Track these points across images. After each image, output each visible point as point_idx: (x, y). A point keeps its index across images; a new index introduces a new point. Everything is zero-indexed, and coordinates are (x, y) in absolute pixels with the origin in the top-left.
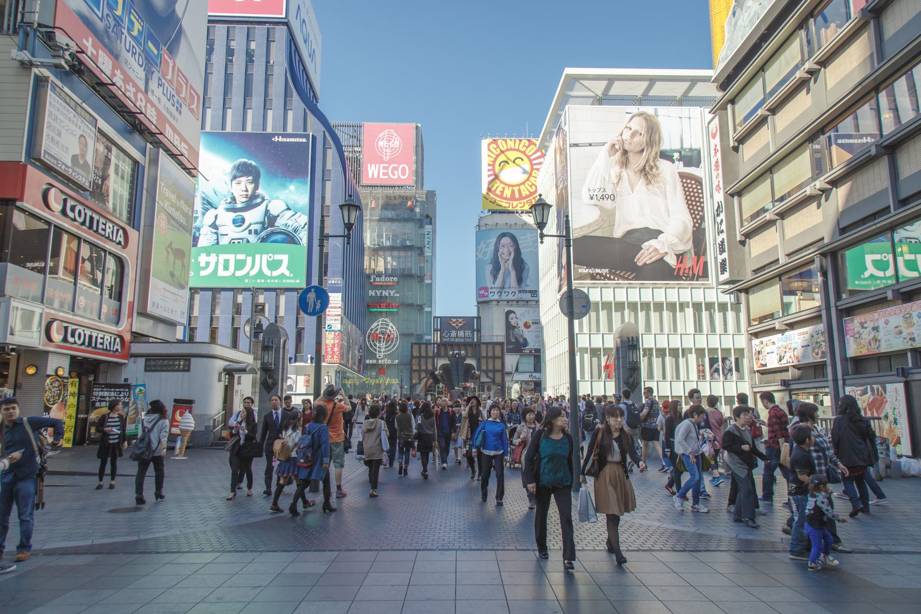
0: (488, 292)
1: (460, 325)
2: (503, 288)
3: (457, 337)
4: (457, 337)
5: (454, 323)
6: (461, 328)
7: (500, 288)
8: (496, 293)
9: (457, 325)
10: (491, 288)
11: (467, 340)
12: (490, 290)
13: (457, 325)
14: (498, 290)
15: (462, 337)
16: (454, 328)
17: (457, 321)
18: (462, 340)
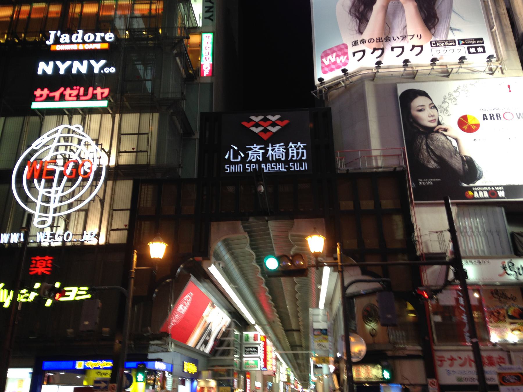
0: (346, 54)
1: (274, 130)
2: (388, 39)
3: (266, 160)
4: (266, 160)
5: (257, 125)
6: (275, 139)
7: (379, 40)
8: (369, 51)
9: (265, 131)
10: (356, 43)
11: (296, 167)
12: (351, 50)
13: (265, 131)
14: (375, 45)
15: (278, 161)
16: (257, 139)
17: (265, 120)
18: (281, 168)
